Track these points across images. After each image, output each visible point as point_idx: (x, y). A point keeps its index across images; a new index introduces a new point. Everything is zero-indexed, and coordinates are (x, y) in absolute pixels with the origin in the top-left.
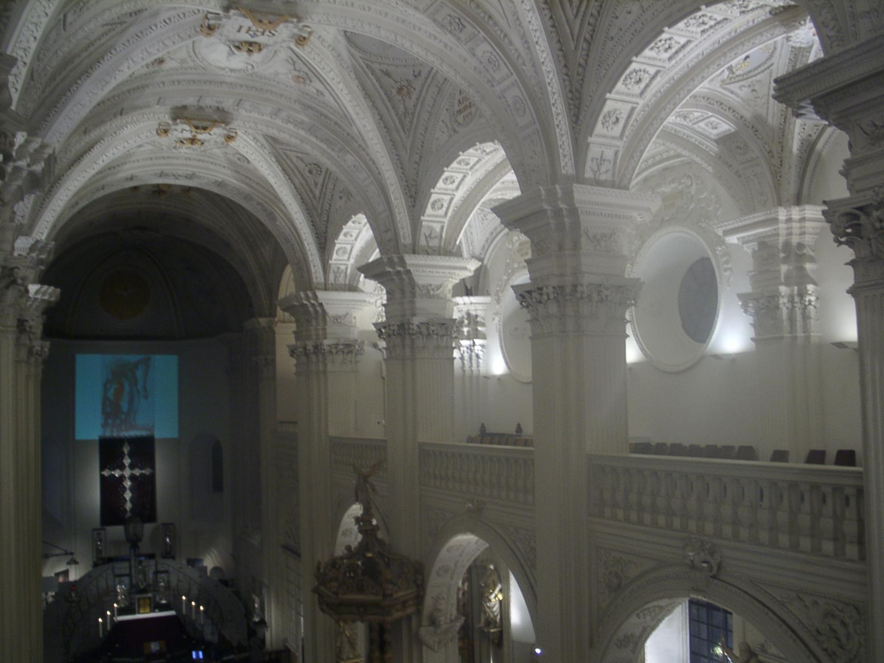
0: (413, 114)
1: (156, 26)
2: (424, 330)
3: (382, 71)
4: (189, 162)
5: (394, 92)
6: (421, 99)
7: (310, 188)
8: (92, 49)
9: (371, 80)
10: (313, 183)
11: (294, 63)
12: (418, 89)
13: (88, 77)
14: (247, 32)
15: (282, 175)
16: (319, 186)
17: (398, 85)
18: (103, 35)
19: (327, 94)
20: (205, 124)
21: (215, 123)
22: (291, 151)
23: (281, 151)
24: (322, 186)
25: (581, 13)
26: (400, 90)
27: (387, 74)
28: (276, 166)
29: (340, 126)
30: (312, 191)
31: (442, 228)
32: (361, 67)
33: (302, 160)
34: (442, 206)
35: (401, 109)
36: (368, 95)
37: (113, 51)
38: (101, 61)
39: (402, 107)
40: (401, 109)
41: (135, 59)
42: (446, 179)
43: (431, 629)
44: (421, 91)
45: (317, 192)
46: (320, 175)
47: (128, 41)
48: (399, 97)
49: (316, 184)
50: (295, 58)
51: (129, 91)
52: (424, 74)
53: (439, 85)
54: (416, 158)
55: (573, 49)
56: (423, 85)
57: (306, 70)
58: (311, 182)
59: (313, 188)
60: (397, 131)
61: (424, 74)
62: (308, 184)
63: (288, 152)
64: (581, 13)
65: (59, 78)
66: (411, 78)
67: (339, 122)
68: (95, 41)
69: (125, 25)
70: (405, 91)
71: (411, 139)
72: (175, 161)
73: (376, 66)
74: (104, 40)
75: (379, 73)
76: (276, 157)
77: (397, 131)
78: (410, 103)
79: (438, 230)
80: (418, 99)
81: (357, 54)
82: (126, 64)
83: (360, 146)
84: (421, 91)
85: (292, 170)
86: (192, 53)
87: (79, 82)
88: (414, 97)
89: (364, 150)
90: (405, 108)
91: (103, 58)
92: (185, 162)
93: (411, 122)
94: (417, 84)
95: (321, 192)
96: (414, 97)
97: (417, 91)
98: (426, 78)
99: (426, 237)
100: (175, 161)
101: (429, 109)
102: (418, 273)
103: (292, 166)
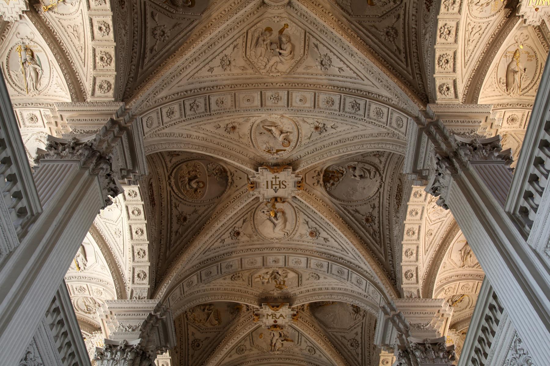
0: (380, 232)
1: (230, 202)
3: (354, 211)
4: (280, 361)
5: (364, 221)
6: (381, 223)
7: (354, 357)
8: (200, 218)
9: (349, 217)
10: (355, 354)
11: (307, 223)
12: (377, 216)
13: (199, 234)
14: (272, 188)
15: (335, 351)
16: (360, 355)
17: (364, 218)
18: (205, 211)
19: (330, 239)
20: (277, 304)
21: (283, 304)
22: (337, 332)
23: (330, 333)
24: (362, 354)
25: (409, 64)
26: (367, 220)
27: (357, 211)
28: (329, 343)
29: (342, 259)
30: (356, 360)
31: (418, 291)
32: (342, 210)
33: (345, 338)
34: (412, 275)
35: (372, 231)
36: (350, 227)
37: (211, 219)
38: (205, 225)
39: (372, 230)
40: (372, 231)
42: (406, 252)
44: (379, 217)
45: (359, 359)
46: (358, 346)
47: (218, 213)
48: (368, 225)
49: (358, 354)
50: (308, 219)
51: (224, 255)
52: (377, 205)
53: (387, 209)
54: (390, 258)
55: (412, 78)
56: (379, 212)
57: (314, 225)
58: (354, 353)
59: (356, 357)
60: (373, 244)
61: (377, 205)
62: (352, 355)
63: (335, 333)
64: (409, 64)
65: (184, 236)
66: (371, 210)
67: (342, 256)
68: (202, 214)
69: (215, 204)
70: (370, 220)
71: (383, 248)
72: (272, 361)
73: (350, 208)
74: (206, 213)
75: (352, 212)
76: (328, 338)
77: (373, 244)
78: (376, 227)
79: (416, 293)
80: (379, 222)
81: (337, 202)
82: (216, 223)
83: (356, 266)
84: (379, 217)
85: (340, 345)
86: (254, 229)
87: (194, 236)
88: (376, 222)
89: (359, 267)
90: (373, 229)
91: (206, 223)
92: (279, 361)
93: (380, 237)
94: (375, 214)
95: (362, 359)
96: (376, 222)
97: (377, 218)
98: (379, 207)
100: (272, 361)
101: (388, 227)
103: (339, 342)
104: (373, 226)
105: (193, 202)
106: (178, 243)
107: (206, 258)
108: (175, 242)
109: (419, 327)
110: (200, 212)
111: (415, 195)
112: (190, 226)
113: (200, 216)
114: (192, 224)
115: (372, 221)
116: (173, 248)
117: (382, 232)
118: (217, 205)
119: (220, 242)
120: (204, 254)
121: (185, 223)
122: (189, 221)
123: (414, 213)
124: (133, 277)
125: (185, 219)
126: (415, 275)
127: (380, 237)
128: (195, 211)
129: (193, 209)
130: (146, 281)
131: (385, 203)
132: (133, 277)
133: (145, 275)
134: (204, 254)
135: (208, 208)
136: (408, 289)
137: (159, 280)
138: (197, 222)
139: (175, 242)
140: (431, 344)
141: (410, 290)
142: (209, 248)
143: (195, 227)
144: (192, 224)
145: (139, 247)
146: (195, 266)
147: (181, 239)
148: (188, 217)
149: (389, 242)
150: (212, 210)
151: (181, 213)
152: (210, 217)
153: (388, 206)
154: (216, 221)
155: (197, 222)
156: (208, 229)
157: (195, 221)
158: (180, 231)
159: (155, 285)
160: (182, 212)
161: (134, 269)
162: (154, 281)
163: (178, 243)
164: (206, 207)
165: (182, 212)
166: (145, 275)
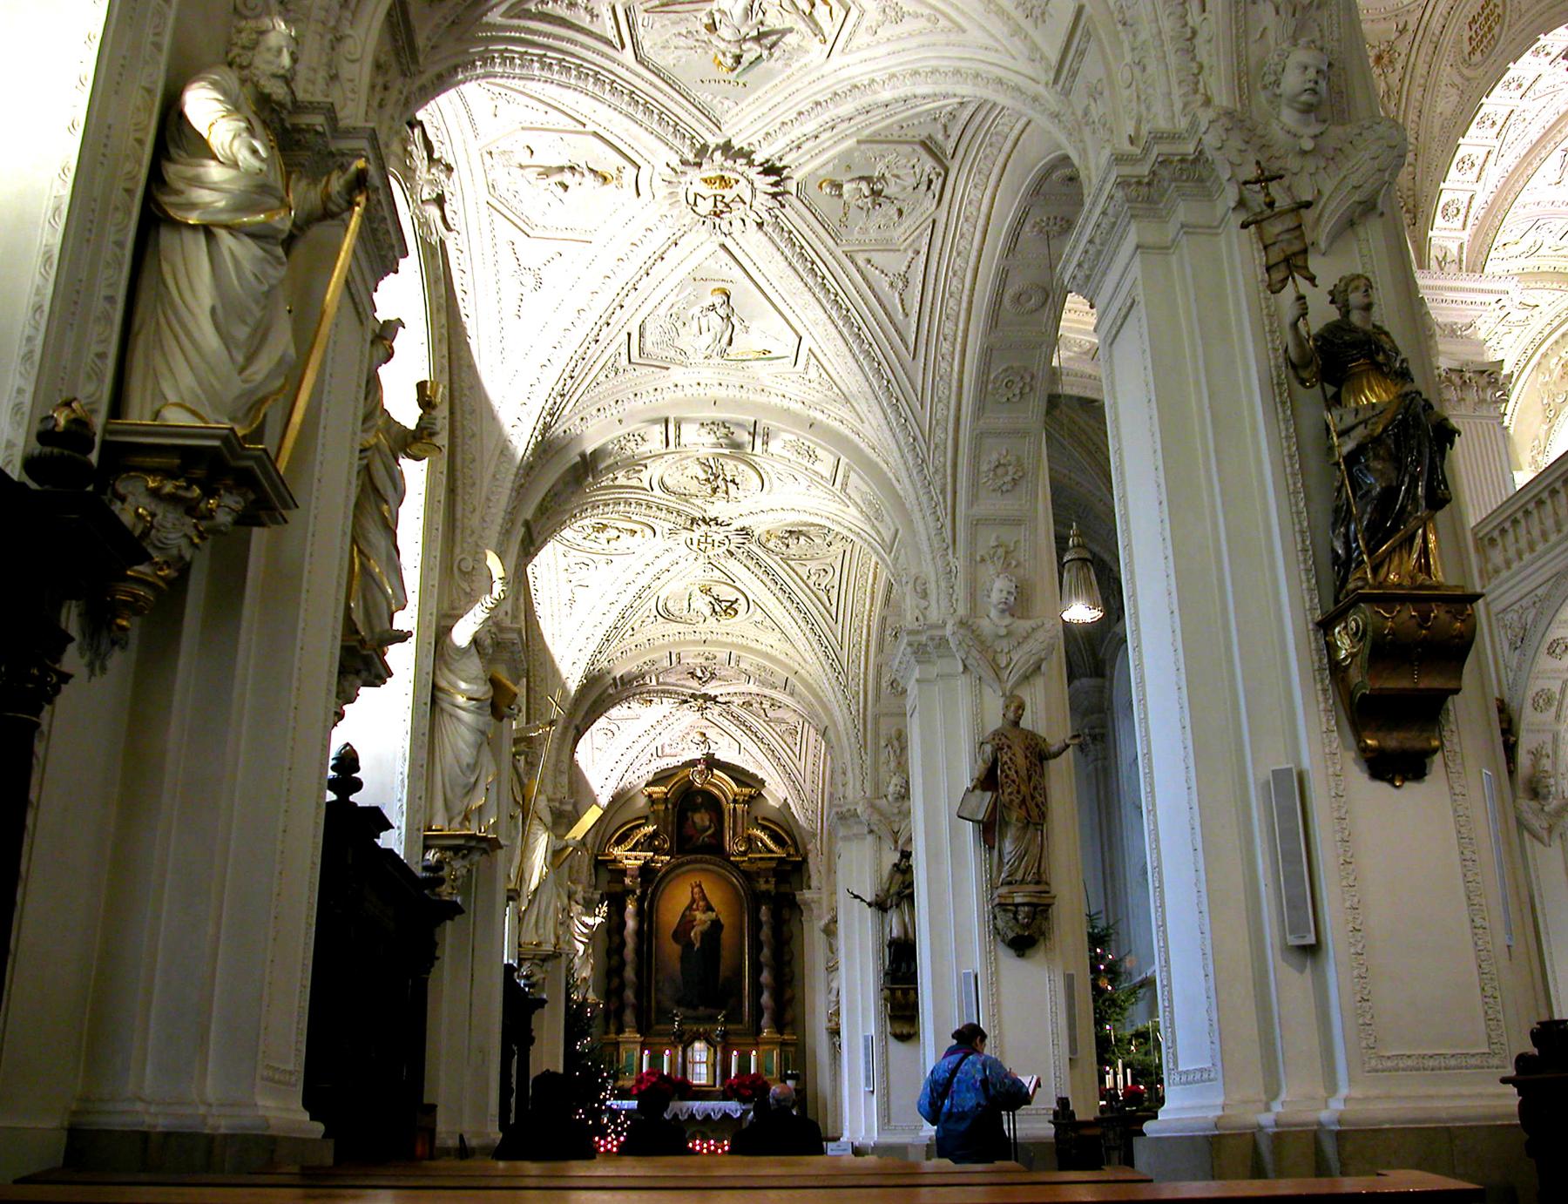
0: (1399, 93)
2: (1454, 377)
26: (1379, 58)
34: (1458, 210)
43: (1534, 804)
44: (1409, 56)
52: (1411, 27)
70: (1385, 60)
78: (1394, 78)
84: (1409, 56)
88: (1399, 66)
93: (1397, 105)
94: (1402, 47)
96: (1399, 66)
97: (1403, 55)
99: (1439, 263)
102: (1435, 304)
104: (1390, 75)
109: (1453, 331)
111: (1537, 53)
115: (1390, 62)
117: (1404, 93)
123: (1513, 86)
126: (1463, 211)
127: (1397, 105)
131: (1433, 24)
136: (1440, 242)
140: (1474, 372)
141: (1445, 244)
149: (1416, 119)
153: (1437, 33)
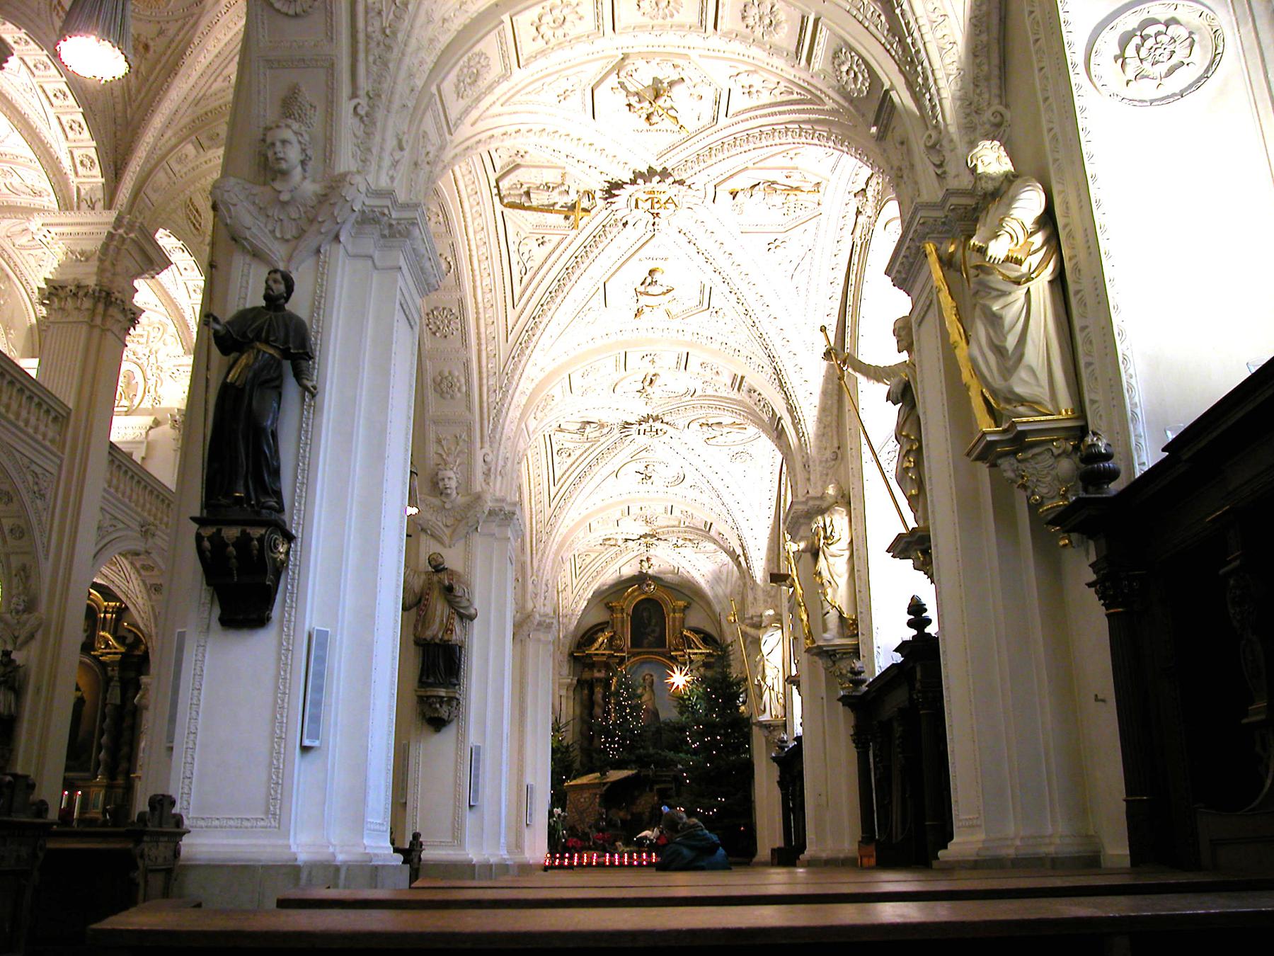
1: (221, 12)
8: (173, 46)
13: (176, 74)
37: (192, 46)
38: (184, 57)
41: (209, 48)
65: (152, 78)
82: (202, 56)
87: (169, 80)
105: (154, 14)
106: (143, 94)
107: (203, 111)
108: (139, 92)
110: (171, 33)
112: (158, 61)
113: (172, 41)
114: (161, 56)
116: (137, 103)
118: (199, 18)
119: (223, 81)
120: (196, 105)
121: (148, 56)
122: (155, 52)
124: (75, 166)
125: (146, 47)
128: (161, 32)
129: (154, 28)
130: (97, 171)
132: (75, 166)
133: (92, 162)
134: (196, 105)
135: (184, 25)
137: (122, 164)
138: (169, 52)
139: (139, 92)
142: (204, 95)
143: (167, 61)
144: (161, 56)
145: (69, 117)
146: (185, 127)
147: (148, 85)
148: (151, 43)
150: (192, 27)
151: (136, 36)
152: (189, 42)
154: (202, 50)
155: (169, 52)
156: (190, 67)
157: (166, 50)
158: (143, 69)
159: (116, 174)
160: (139, 35)
161: (71, 153)
162: (112, 168)
163: (143, 94)
164: (180, 23)
165: (139, 35)
166: (92, 162)
